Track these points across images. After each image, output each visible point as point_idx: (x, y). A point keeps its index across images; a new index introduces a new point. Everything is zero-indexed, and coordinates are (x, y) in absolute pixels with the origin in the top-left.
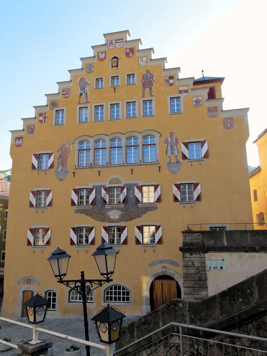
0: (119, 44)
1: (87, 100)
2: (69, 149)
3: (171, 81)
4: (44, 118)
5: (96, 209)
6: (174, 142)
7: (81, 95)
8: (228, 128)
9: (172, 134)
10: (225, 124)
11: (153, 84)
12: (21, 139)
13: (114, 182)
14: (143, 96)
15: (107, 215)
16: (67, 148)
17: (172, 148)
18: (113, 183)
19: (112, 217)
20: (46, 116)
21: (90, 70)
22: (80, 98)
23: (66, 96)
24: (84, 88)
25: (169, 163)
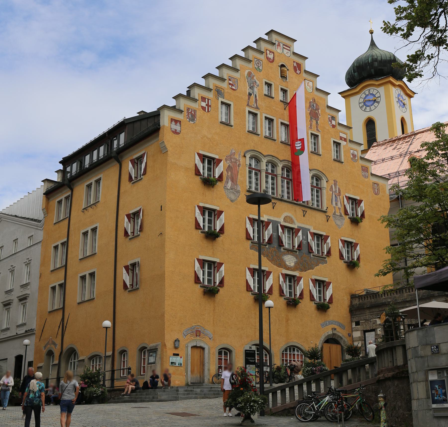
1: (257, 105)
2: (239, 161)
3: (334, 122)
4: (206, 105)
7: (250, 94)
9: (335, 182)
12: (178, 124)
15: (283, 259)
18: (287, 222)
19: (287, 263)
21: (259, 67)
22: (249, 99)
23: (233, 88)
24: (252, 87)
25: (334, 214)
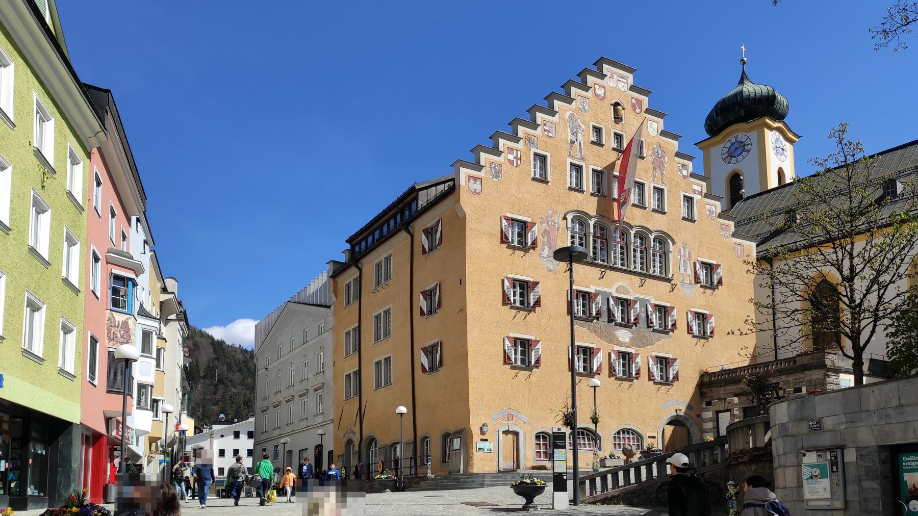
12: (478, 182)
25: (683, 282)
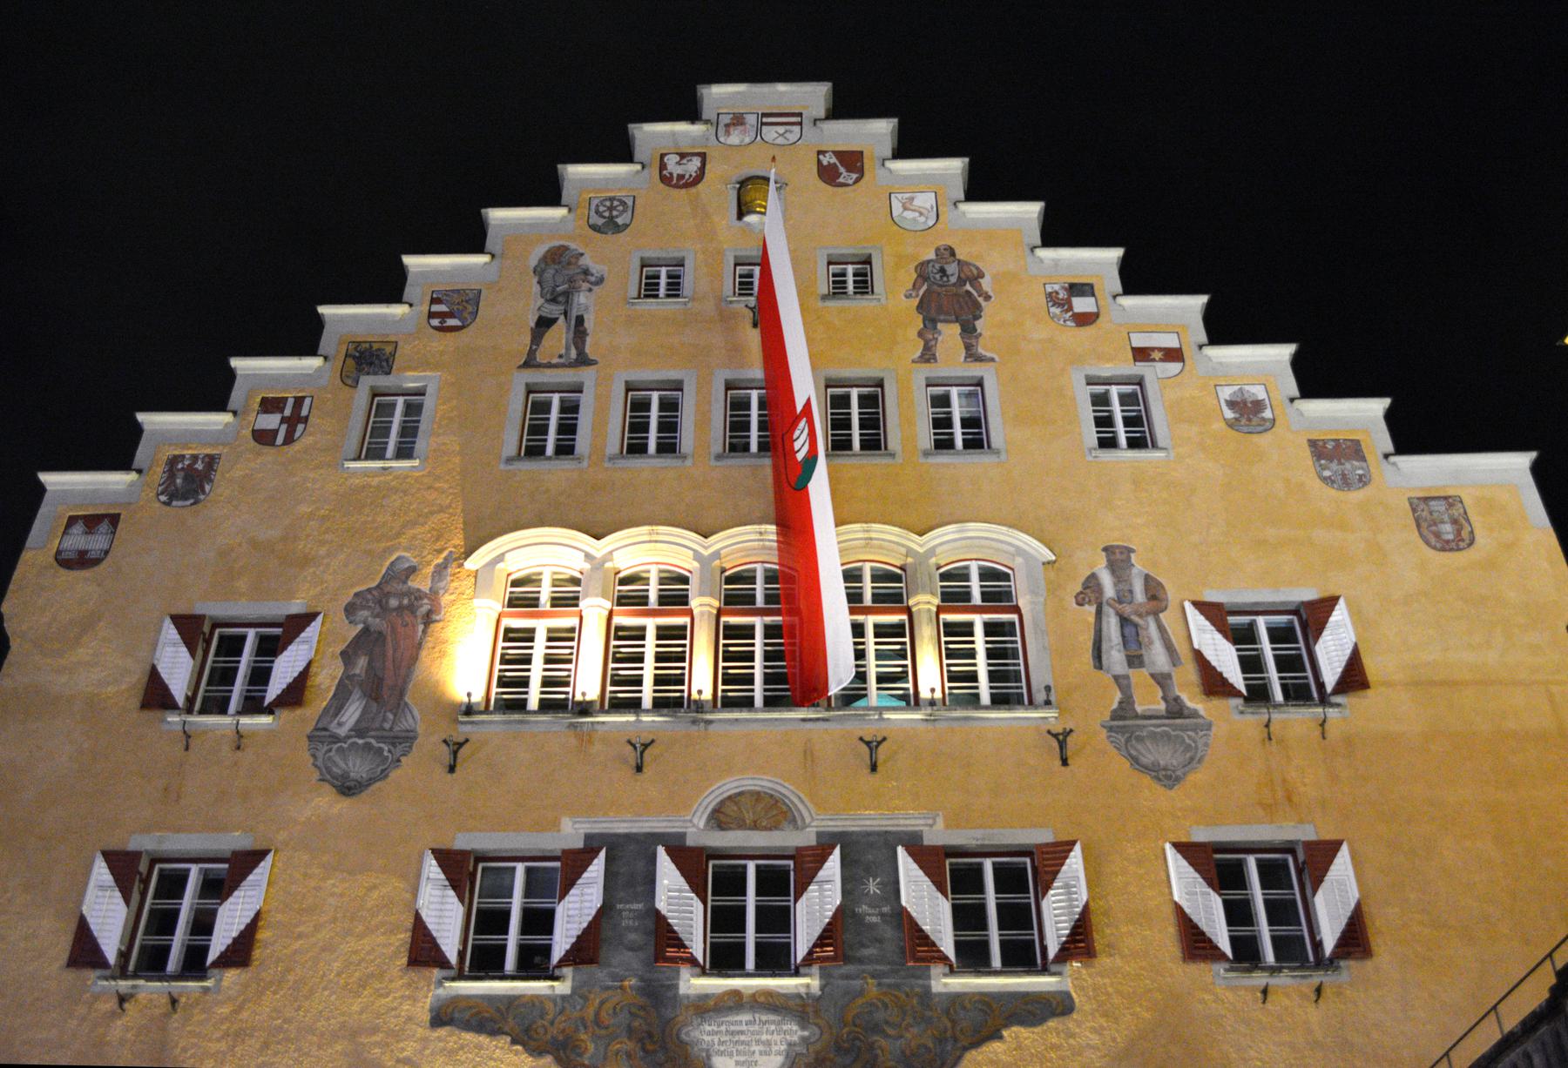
0: (781, 129)
3: (1082, 305)
4: (283, 420)
5: (602, 1003)
6: (1140, 596)
7: (544, 323)
8: (1446, 547)
9: (1118, 559)
10: (1424, 525)
11: (978, 307)
12: (104, 526)
13: (749, 817)
14: (928, 356)
15: (683, 1045)
16: (418, 595)
17: (1129, 630)
18: (742, 825)
20: (304, 412)
23: (451, 322)
24: (567, 295)
25: (1124, 710)
